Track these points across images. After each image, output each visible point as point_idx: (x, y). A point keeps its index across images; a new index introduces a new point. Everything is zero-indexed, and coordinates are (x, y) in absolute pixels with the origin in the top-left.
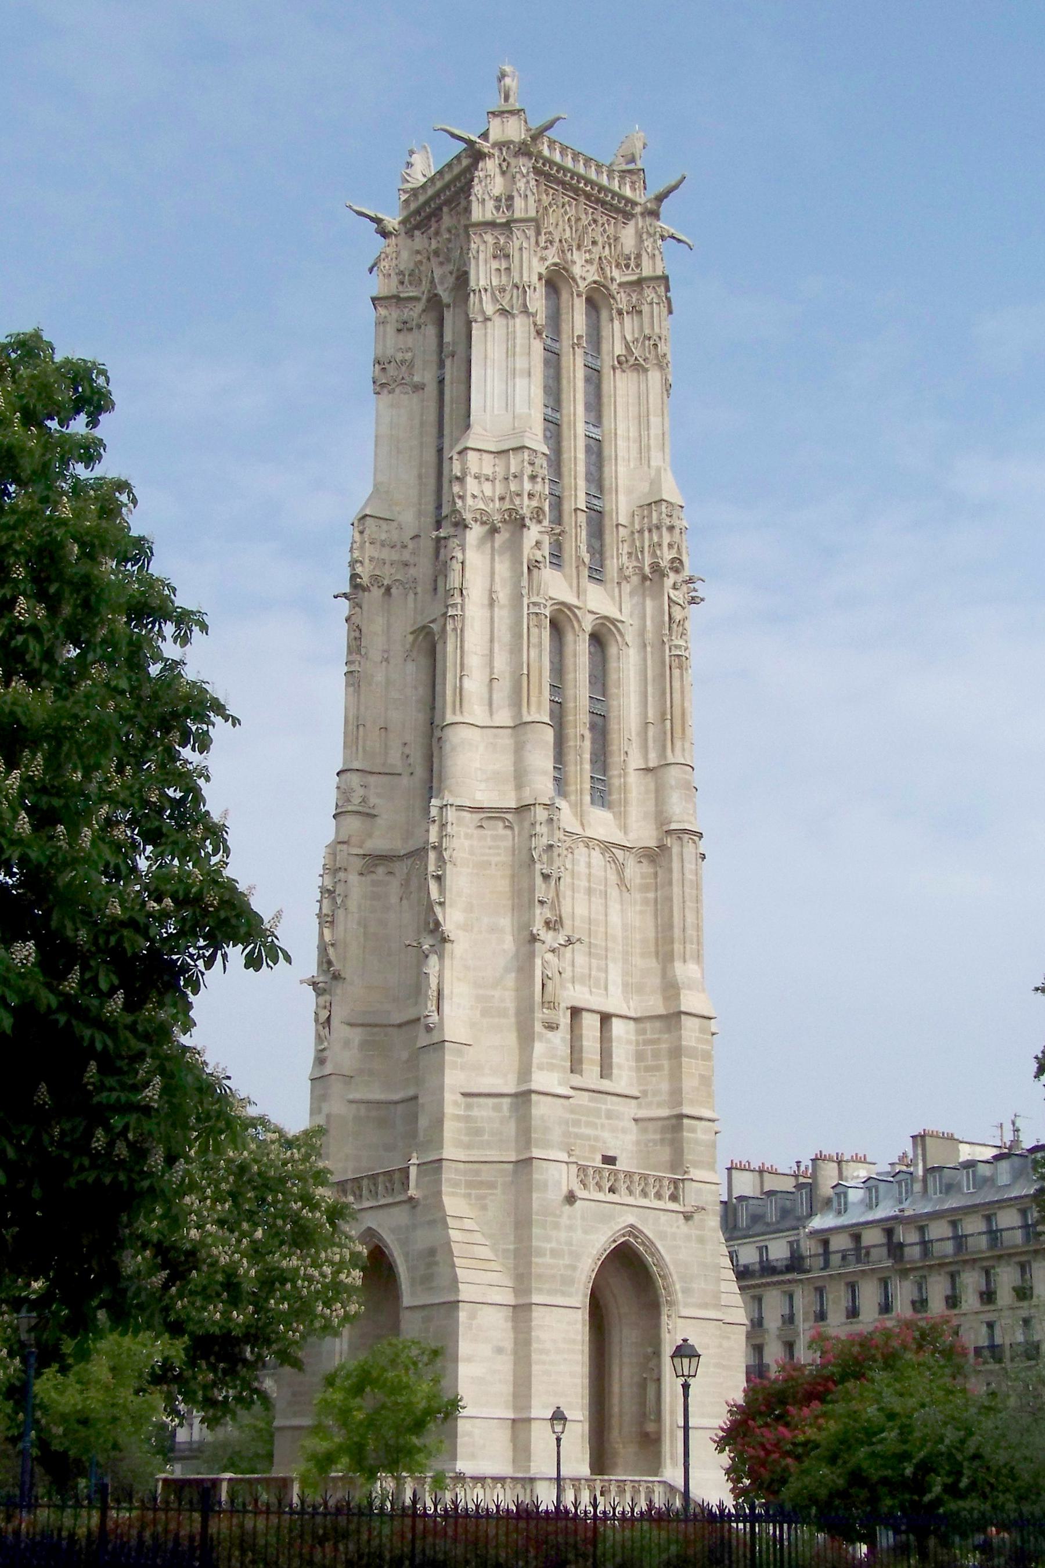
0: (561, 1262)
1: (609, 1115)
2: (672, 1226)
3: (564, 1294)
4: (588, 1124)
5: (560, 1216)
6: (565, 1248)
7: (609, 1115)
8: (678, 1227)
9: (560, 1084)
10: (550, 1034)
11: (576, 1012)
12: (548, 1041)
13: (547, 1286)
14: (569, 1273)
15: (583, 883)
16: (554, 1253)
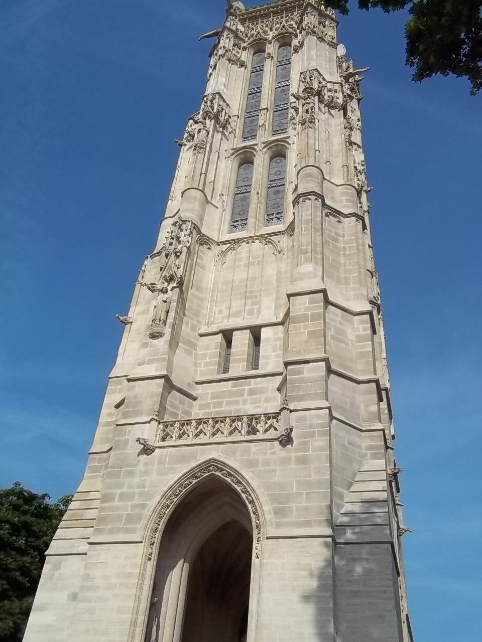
0: (129, 503)
1: (252, 392)
2: (265, 453)
3: (127, 531)
4: (228, 403)
5: (136, 465)
6: (137, 490)
7: (252, 392)
8: (273, 453)
9: (157, 370)
10: (155, 342)
11: (227, 335)
12: (154, 346)
13: (109, 527)
14: (137, 511)
15: (245, 261)
16: (122, 497)
